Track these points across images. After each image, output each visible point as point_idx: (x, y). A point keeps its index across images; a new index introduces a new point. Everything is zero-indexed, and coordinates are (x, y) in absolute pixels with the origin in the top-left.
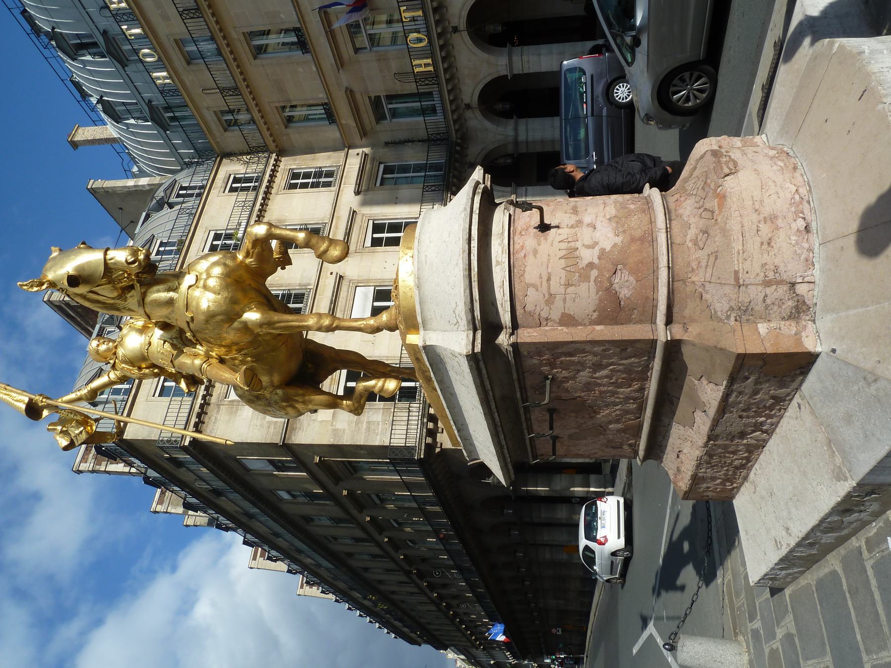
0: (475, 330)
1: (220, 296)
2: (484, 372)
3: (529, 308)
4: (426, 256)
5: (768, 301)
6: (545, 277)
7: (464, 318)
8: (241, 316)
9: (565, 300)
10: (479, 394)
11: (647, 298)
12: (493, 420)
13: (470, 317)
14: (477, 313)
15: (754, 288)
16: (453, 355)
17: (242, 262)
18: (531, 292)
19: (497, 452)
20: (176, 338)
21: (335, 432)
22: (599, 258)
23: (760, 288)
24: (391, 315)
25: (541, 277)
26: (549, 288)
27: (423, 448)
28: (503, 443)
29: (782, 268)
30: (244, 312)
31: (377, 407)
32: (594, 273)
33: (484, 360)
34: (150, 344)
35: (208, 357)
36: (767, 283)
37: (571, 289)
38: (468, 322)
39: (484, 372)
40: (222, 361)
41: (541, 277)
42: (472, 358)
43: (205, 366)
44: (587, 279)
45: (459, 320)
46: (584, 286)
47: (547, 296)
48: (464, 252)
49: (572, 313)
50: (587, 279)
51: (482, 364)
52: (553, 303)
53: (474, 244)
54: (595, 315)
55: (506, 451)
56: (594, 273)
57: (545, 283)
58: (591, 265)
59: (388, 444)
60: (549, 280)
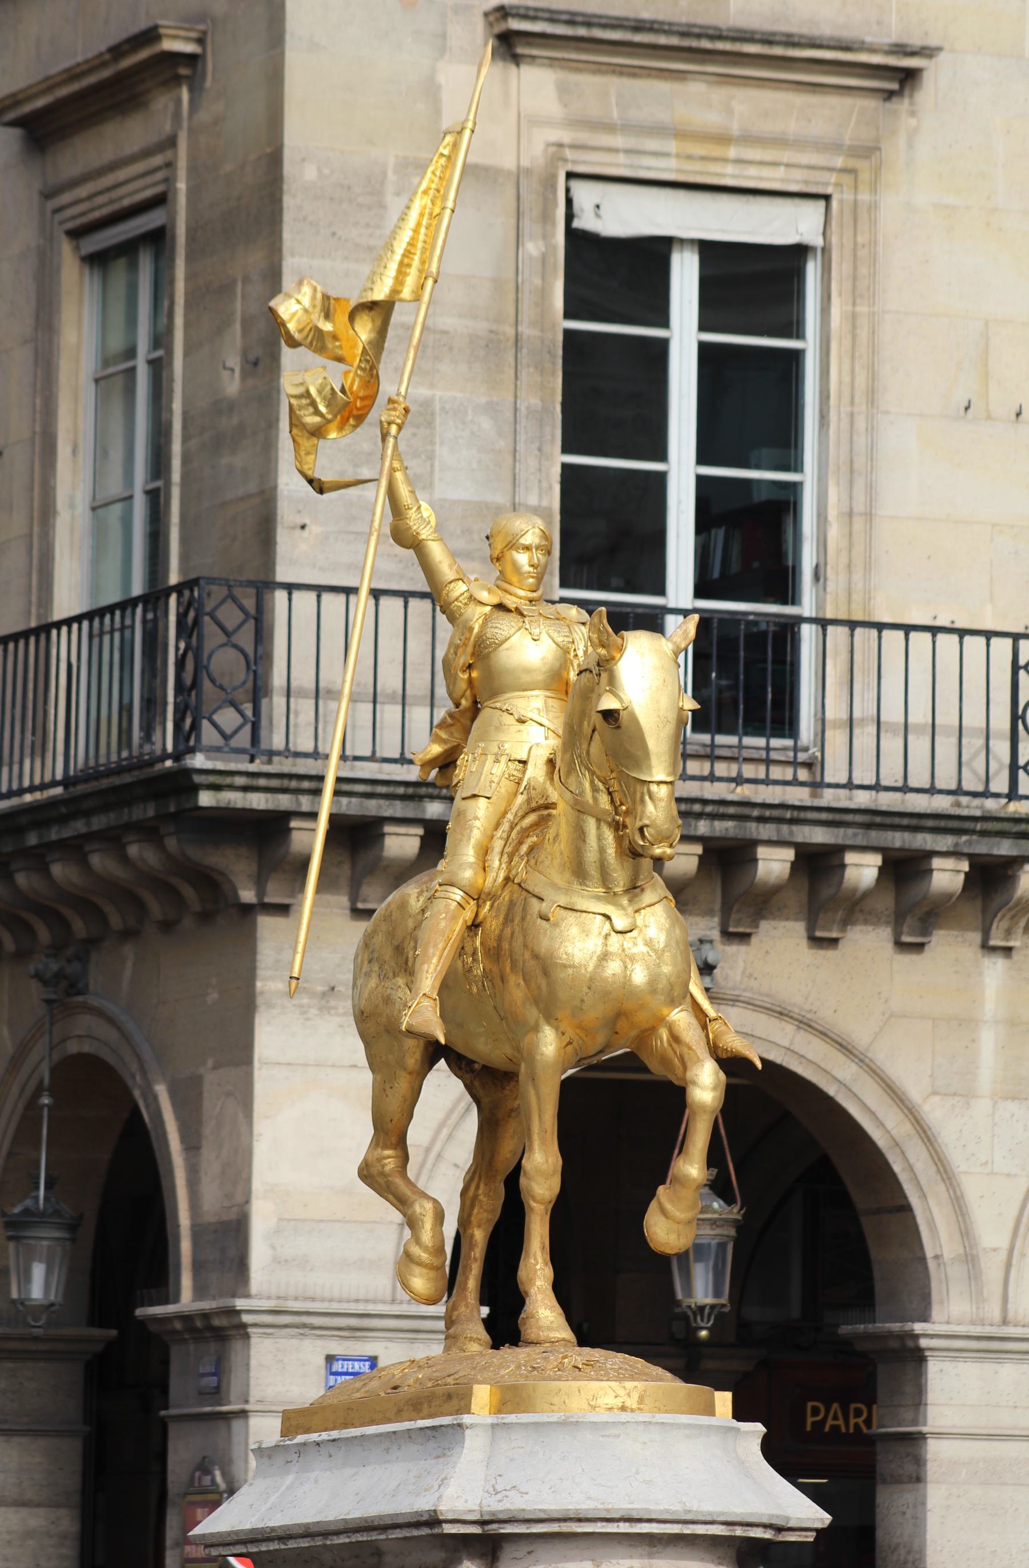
0: (482, 1523)
1: (585, 989)
2: (415, 1533)
4: (618, 1436)
7: (500, 1507)
8: (549, 1023)
10: (380, 1517)
12: (337, 1533)
13: (501, 1516)
14: (508, 1529)
16: (443, 1482)
17: (662, 1020)
19: (273, 1529)
20: (529, 801)
21: (366, 196)
24: (549, 1329)
27: (258, 801)
28: (292, 1544)
30: (557, 1028)
31: (529, 462)
33: (433, 1535)
34: (521, 721)
35: (478, 897)
38: (493, 1514)
39: (415, 1533)
40: (474, 926)
42: (433, 1521)
43: (457, 895)
45: (499, 1497)
48: (608, 1510)
51: (425, 1531)
53: (624, 1528)
55: (273, 1546)
59: (283, 573)
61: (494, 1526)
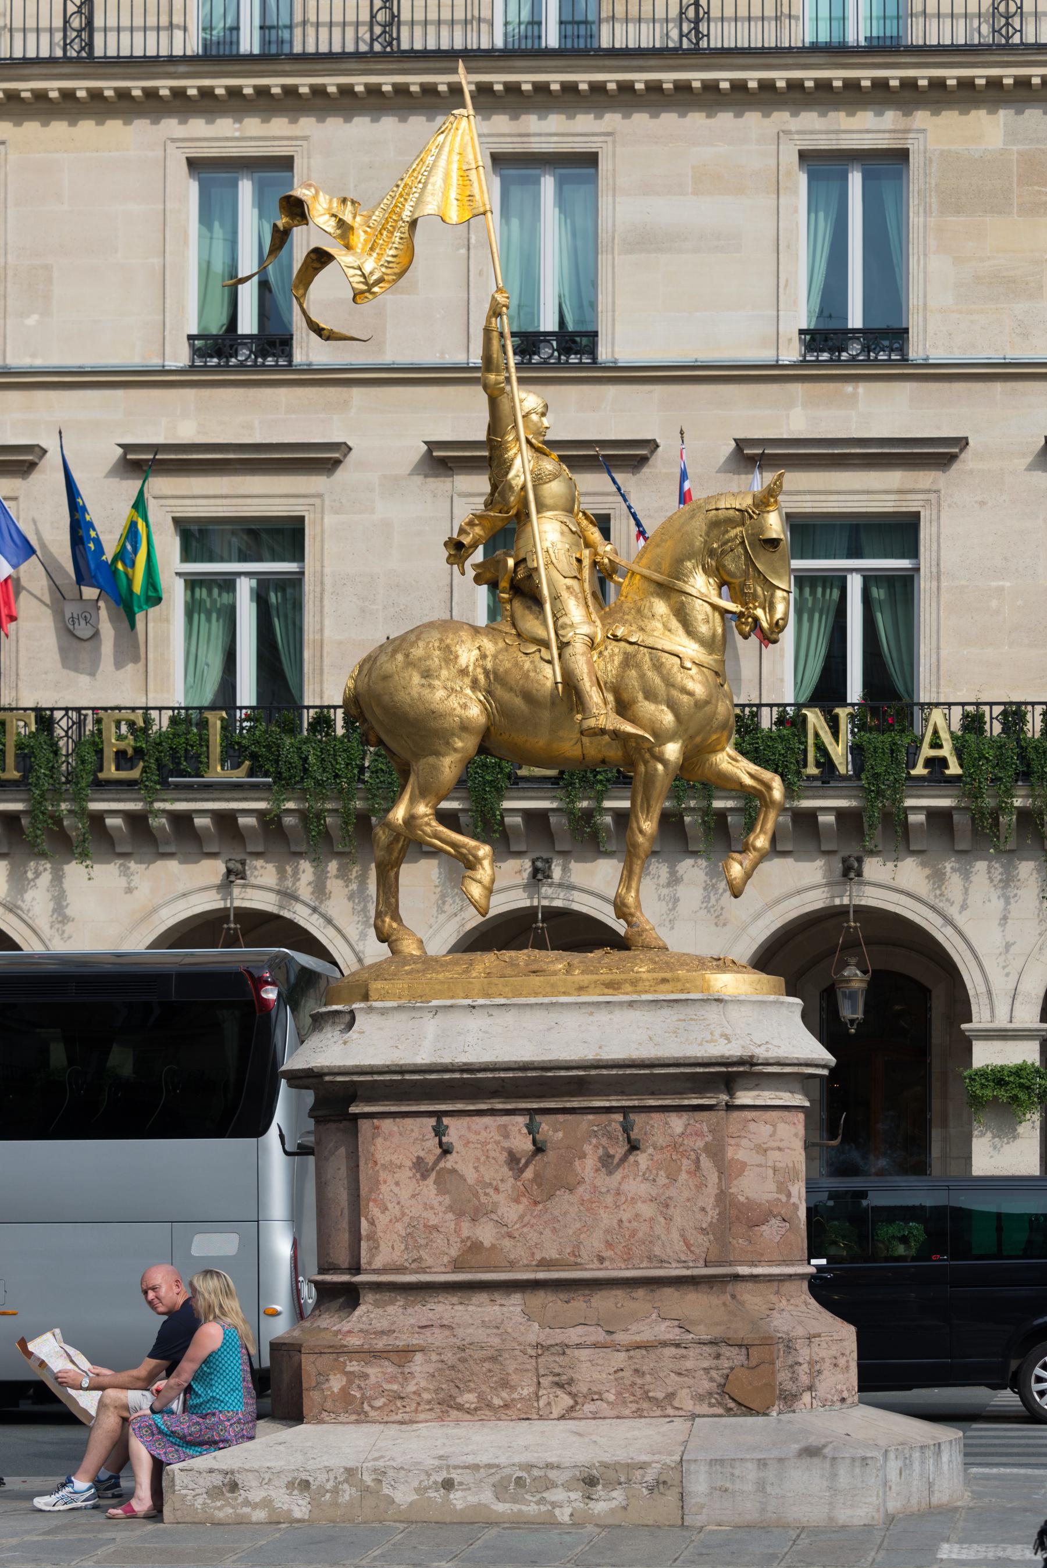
3: (752, 1126)
5: (796, 1367)
6: (781, 1145)
9: (760, 1166)
11: (762, 1255)
13: (771, 1061)
15: (808, 1351)
18: (769, 1128)
22: (794, 1204)
23: (808, 1358)
25: (782, 1140)
26: (772, 1149)
29: (822, 1377)
32: (784, 1198)
36: (811, 1363)
37: (770, 1172)
38: (766, 1059)
41: (782, 1140)
44: (779, 1191)
46: (773, 1187)
47: (765, 1146)
49: (745, 1173)
50: (779, 1191)
52: (758, 1152)
54: (742, 1199)
56: (784, 1198)
57: (775, 1144)
58: (789, 1195)
60: (780, 1149)
61: (760, 1067)
